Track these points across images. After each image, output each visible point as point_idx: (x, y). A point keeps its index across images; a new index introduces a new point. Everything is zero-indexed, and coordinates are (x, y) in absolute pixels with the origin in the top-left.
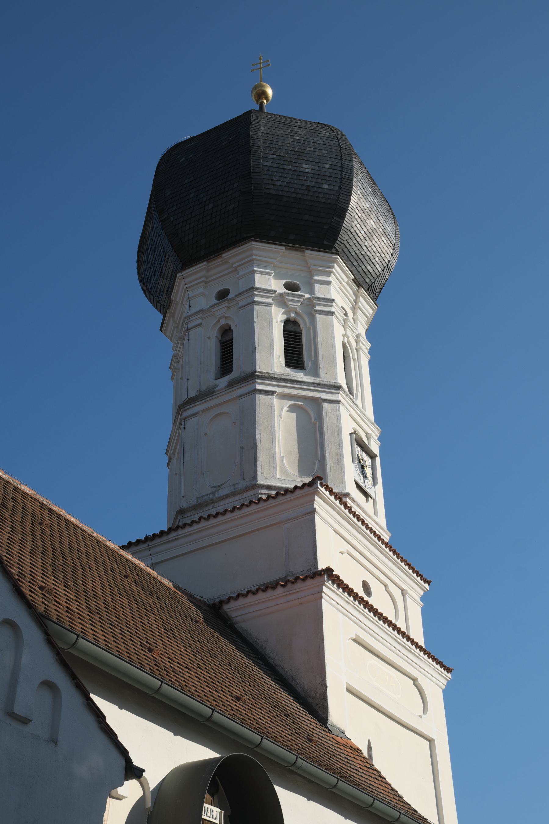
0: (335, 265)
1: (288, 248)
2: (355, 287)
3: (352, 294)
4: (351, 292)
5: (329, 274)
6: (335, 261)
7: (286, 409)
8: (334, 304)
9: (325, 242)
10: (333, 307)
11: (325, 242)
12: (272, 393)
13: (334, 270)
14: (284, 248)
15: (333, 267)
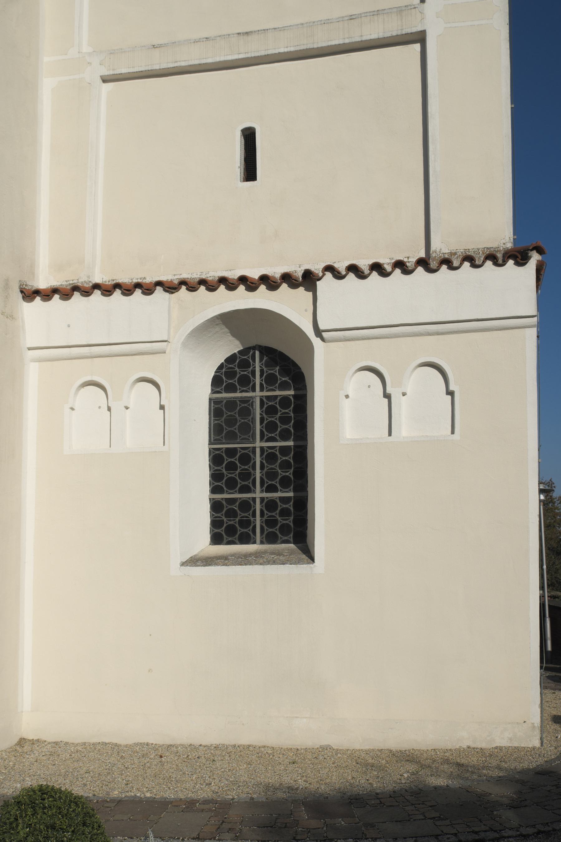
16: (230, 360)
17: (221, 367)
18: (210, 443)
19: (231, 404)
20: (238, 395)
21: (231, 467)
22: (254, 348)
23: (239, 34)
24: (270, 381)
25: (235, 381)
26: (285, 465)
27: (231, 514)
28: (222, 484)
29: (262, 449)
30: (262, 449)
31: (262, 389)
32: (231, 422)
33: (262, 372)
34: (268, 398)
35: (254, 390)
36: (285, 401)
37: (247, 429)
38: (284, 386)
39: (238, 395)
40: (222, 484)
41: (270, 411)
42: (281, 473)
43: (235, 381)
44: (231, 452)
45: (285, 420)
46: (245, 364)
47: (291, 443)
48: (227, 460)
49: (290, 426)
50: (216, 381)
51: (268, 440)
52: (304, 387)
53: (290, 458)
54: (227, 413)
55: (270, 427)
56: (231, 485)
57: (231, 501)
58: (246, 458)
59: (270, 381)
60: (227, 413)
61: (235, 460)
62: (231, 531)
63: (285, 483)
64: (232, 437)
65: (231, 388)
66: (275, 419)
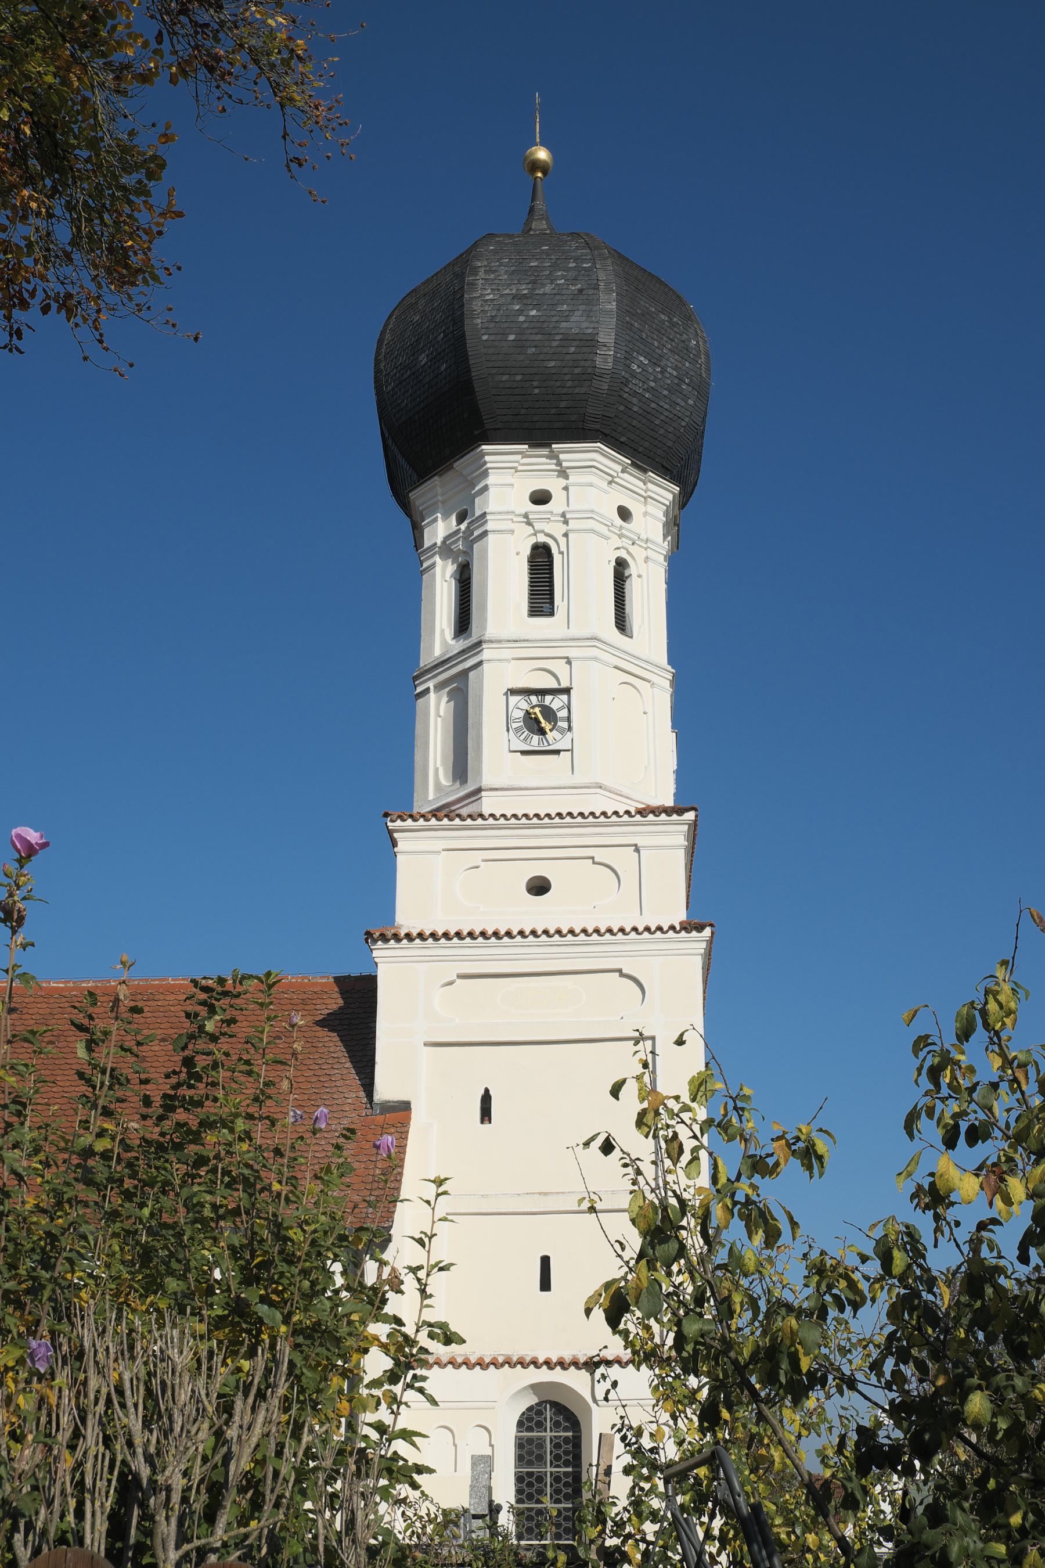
0: (487, 458)
1: (440, 474)
2: (545, 451)
3: (548, 461)
4: (544, 460)
5: (485, 474)
6: (483, 454)
7: (445, 699)
8: (488, 517)
9: (476, 433)
10: (489, 523)
11: (476, 433)
12: (427, 690)
13: (489, 465)
14: (436, 478)
15: (485, 463)
16: (530, 1409)
17: (523, 1414)
18: (516, 1467)
19: (530, 1441)
20: (535, 1434)
21: (530, 1485)
22: (546, 1402)
23: (540, 1194)
24: (557, 1425)
25: (533, 1424)
26: (566, 1484)
27: (530, 1518)
28: (524, 1497)
29: (551, 1473)
30: (551, 1473)
31: (551, 1431)
32: (530, 1453)
33: (551, 1419)
34: (555, 1437)
35: (546, 1431)
36: (566, 1440)
37: (541, 1458)
38: (565, 1429)
39: (535, 1434)
40: (524, 1497)
41: (557, 1446)
42: (564, 1491)
43: (533, 1424)
44: (530, 1474)
45: (566, 1453)
46: (539, 1413)
47: (570, 1469)
48: (527, 1480)
49: (570, 1458)
50: (520, 1424)
51: (556, 1466)
52: (580, 1431)
53: (570, 1480)
54: (527, 1447)
55: (557, 1457)
56: (530, 1497)
57: (530, 1509)
58: (540, 1479)
59: (557, 1425)
60: (527, 1447)
61: (533, 1480)
62: (529, 1530)
63: (567, 1497)
64: (530, 1463)
65: (530, 1429)
66: (560, 1452)
